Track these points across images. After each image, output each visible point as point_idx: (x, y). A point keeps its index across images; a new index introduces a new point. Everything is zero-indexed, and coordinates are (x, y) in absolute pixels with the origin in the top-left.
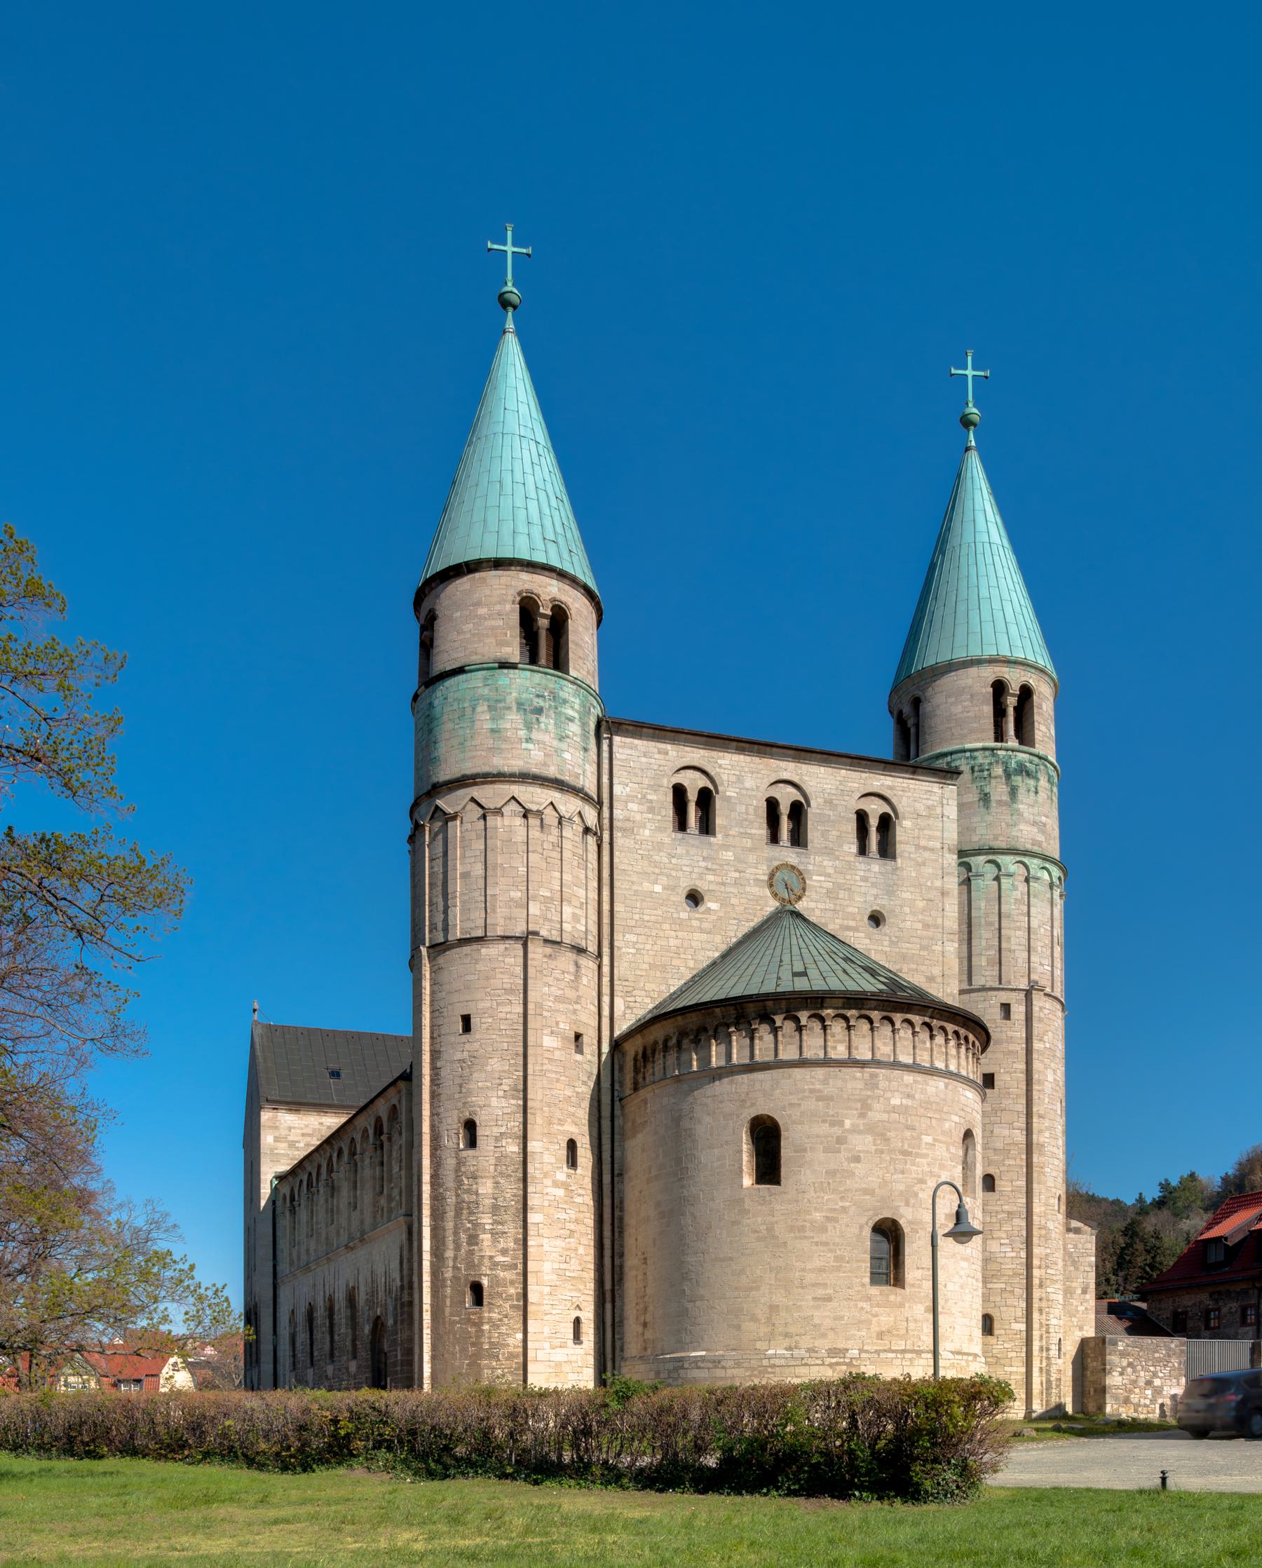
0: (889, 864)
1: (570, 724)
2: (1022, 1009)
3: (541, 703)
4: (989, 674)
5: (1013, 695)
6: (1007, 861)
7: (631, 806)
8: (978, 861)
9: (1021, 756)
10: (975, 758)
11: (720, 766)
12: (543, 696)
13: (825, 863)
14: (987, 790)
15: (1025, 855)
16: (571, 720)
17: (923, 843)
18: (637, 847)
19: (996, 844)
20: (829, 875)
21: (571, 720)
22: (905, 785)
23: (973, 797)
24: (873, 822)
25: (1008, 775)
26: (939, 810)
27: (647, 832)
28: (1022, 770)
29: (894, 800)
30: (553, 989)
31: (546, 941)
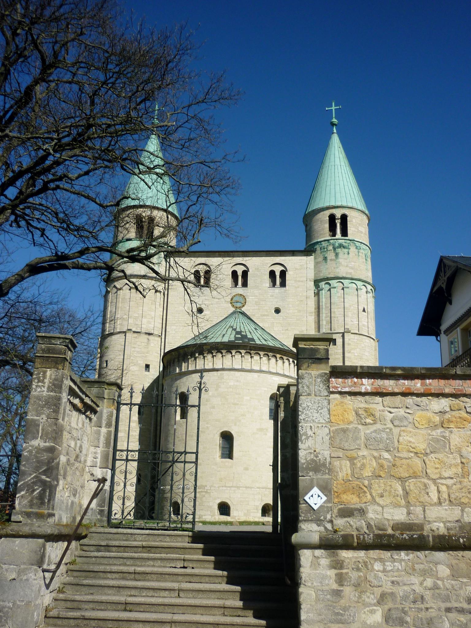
0: (283, 289)
2: (341, 340)
4: (328, 213)
5: (338, 219)
6: (333, 283)
8: (322, 284)
9: (340, 241)
13: (255, 292)
14: (326, 256)
15: (341, 279)
17: (298, 279)
19: (329, 276)
20: (257, 296)
23: (320, 259)
24: (278, 274)
25: (334, 249)
26: (305, 266)
28: (341, 246)
30: (136, 349)
31: (134, 332)
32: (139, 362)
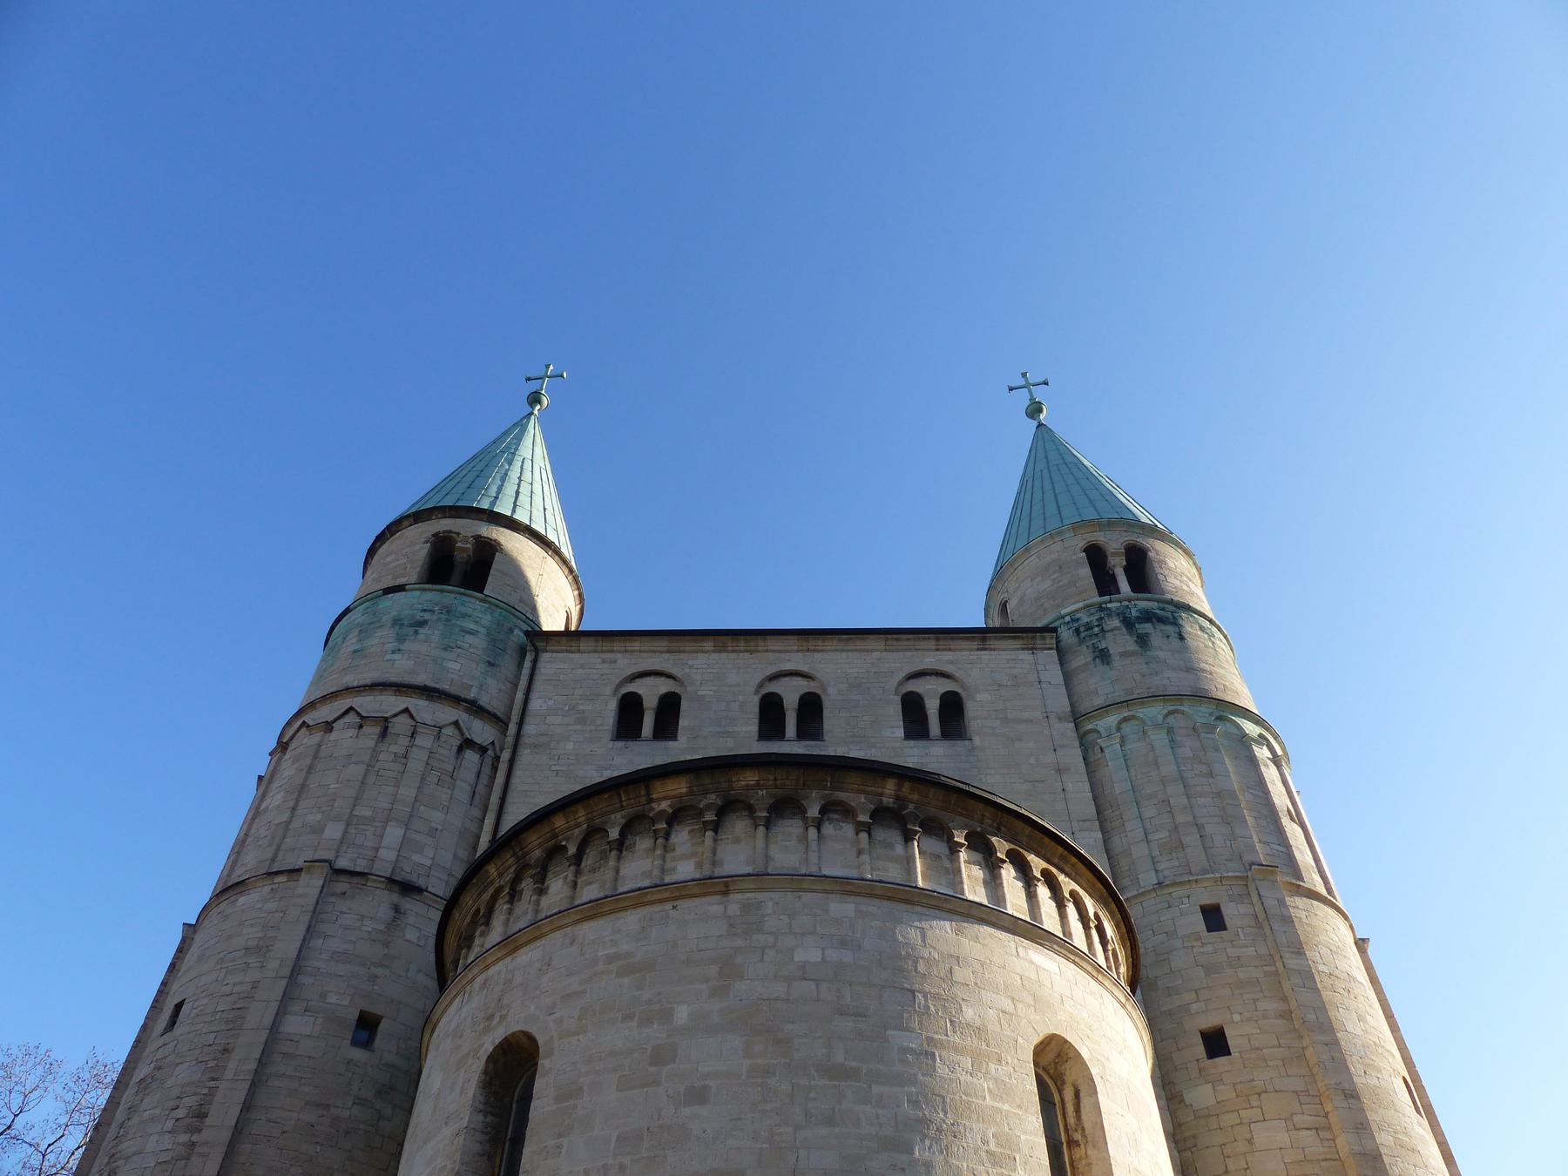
0: (960, 746)
1: (467, 636)
3: (427, 616)
4: (1080, 542)
7: (550, 719)
10: (1077, 620)
11: (691, 667)
12: (432, 611)
14: (1103, 645)
16: (472, 632)
18: (552, 762)
21: (472, 632)
22: (974, 657)
26: (1033, 677)
27: (570, 746)
29: (958, 674)
32: (333, 998)
